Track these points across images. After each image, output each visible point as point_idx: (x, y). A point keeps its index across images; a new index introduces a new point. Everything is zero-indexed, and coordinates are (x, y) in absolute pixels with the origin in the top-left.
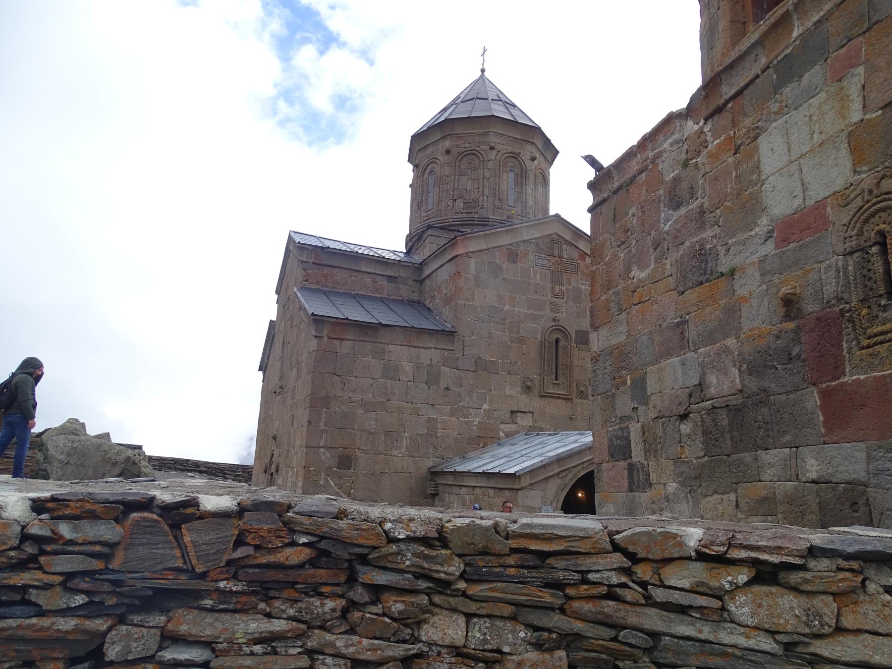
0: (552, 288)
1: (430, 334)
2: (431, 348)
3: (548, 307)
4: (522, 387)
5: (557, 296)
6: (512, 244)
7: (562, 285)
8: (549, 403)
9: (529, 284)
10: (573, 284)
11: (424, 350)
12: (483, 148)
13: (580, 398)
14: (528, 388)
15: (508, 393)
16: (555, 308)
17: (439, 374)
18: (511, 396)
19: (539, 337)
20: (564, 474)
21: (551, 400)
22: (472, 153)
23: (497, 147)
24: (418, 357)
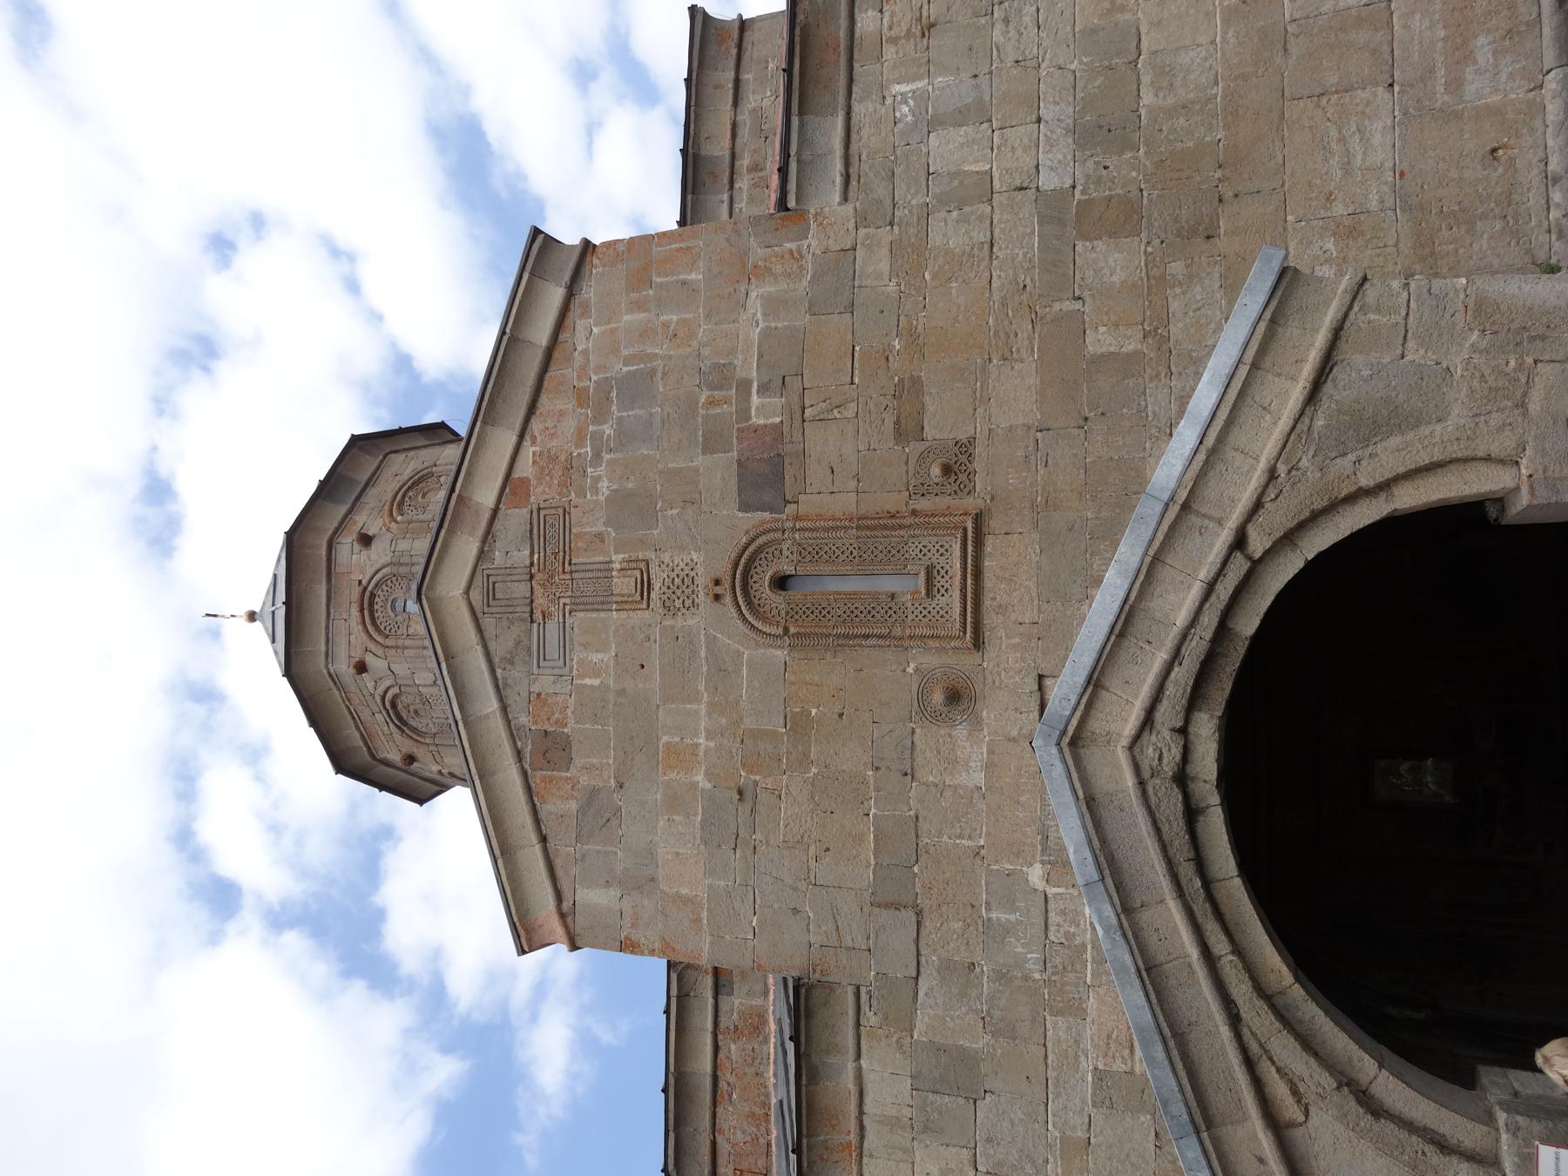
0: (624, 605)
1: (814, 1077)
2: (859, 1070)
3: (679, 622)
4: (952, 723)
5: (645, 586)
6: (519, 755)
7: (607, 567)
8: (1002, 609)
9: (621, 693)
10: (599, 528)
11: (868, 1099)
12: (370, 685)
13: (971, 475)
14: (954, 697)
15: (979, 778)
16: (679, 598)
17: (941, 1049)
18: (989, 767)
19: (780, 655)
20: (1279, 1089)
21: (987, 603)
22: (393, 708)
23: (357, 655)
24: (892, 1123)
